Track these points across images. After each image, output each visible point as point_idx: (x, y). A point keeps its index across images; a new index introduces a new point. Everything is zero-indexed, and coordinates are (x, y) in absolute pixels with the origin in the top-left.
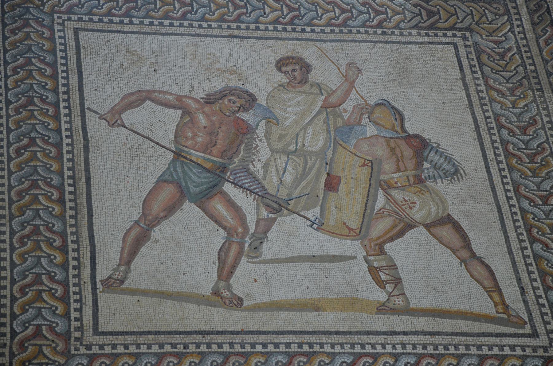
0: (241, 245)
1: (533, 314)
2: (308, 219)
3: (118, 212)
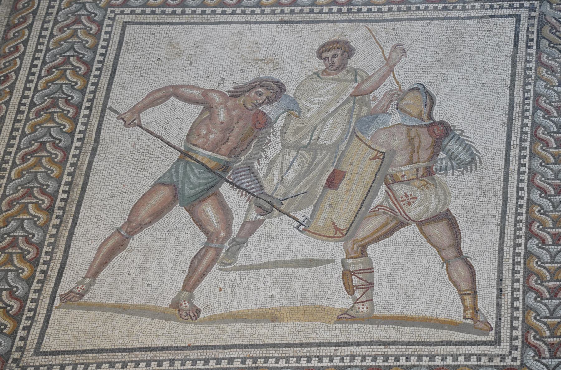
0: (218, 251)
1: (503, 319)
2: (297, 220)
3: (103, 219)
